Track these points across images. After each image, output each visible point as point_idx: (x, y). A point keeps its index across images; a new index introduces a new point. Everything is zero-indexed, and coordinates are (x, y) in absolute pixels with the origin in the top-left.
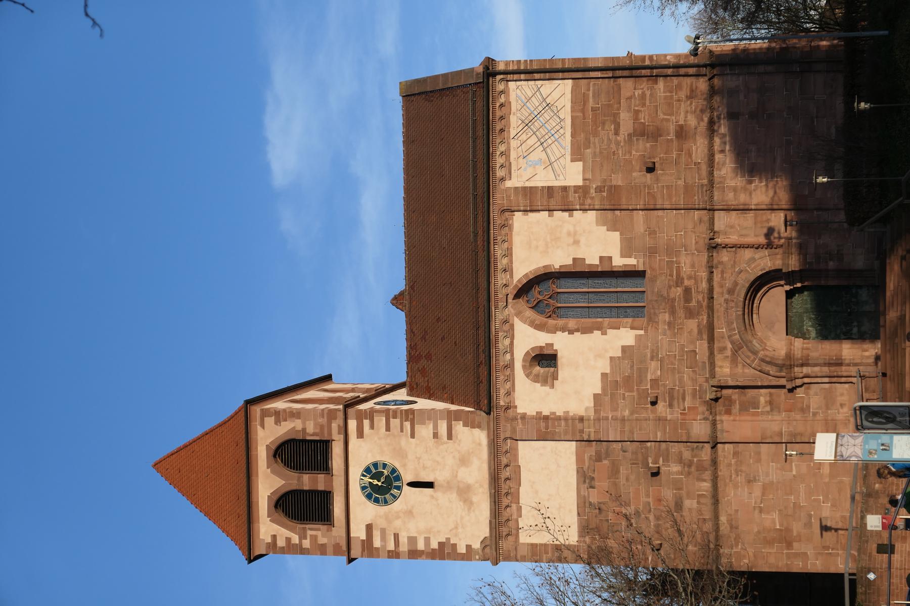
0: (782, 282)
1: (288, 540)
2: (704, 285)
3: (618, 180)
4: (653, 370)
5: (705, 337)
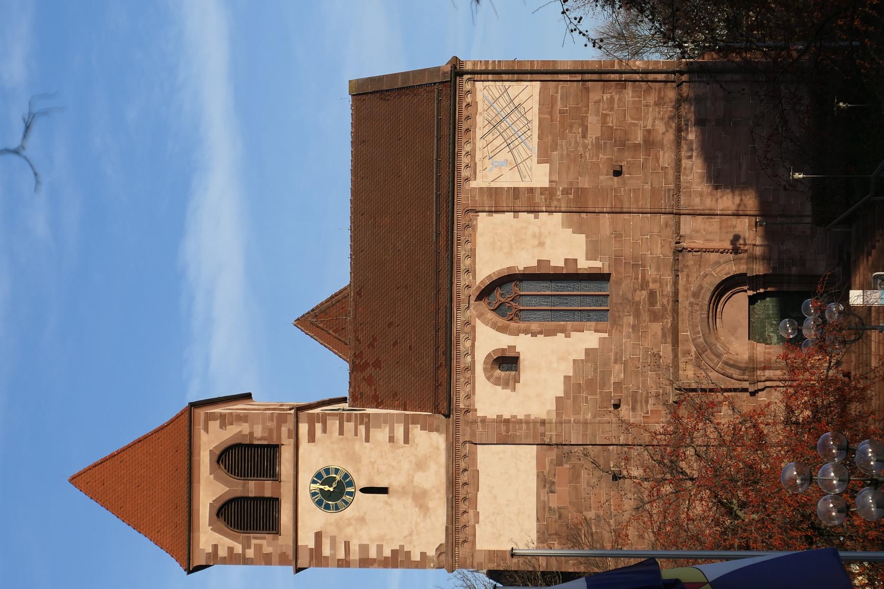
0: (746, 288)
1: (231, 549)
2: (669, 289)
3: (585, 183)
4: (617, 373)
5: (669, 340)
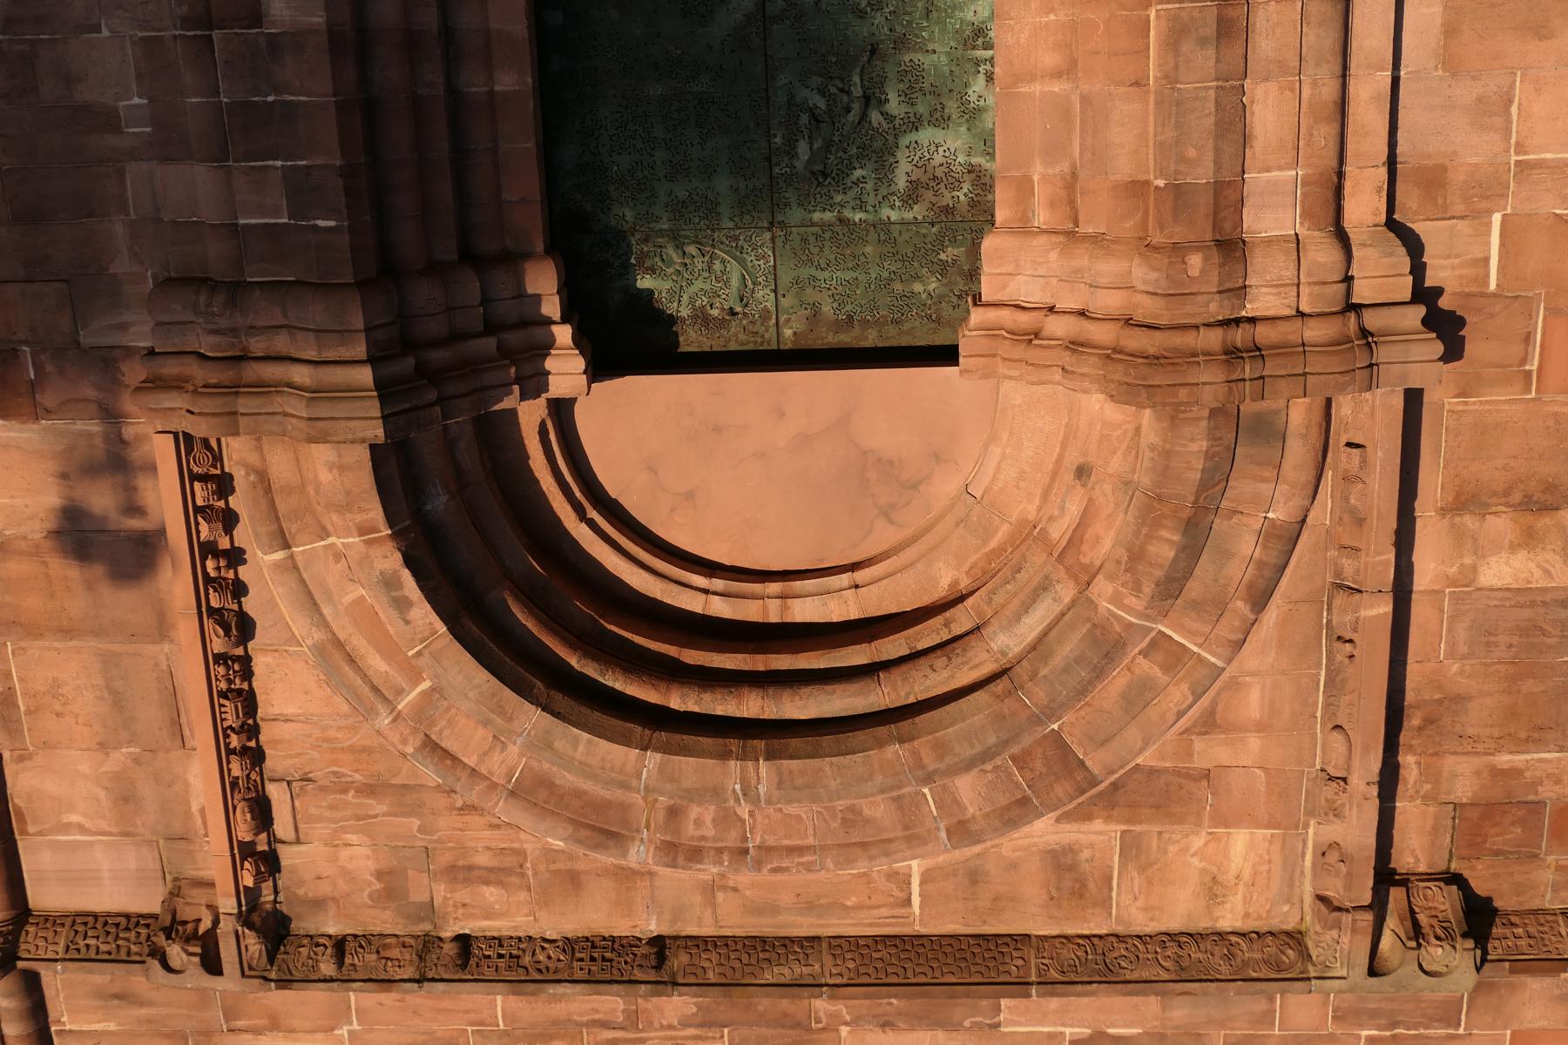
0: (531, 415)
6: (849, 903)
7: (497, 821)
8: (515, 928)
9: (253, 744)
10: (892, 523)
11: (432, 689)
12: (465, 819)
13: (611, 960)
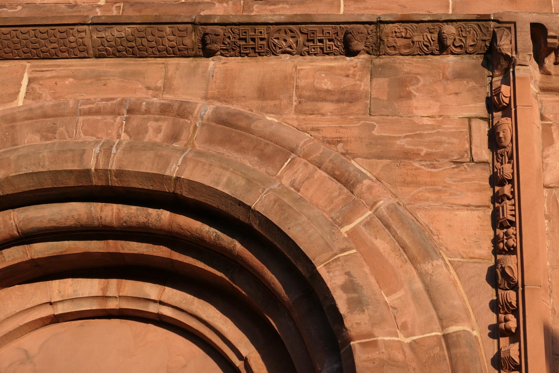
6: (71, 80)
7: (313, 133)
8: (312, 61)
9: (497, 188)
10: (26, 351)
11: (341, 225)
12: (338, 135)
13: (240, 39)
